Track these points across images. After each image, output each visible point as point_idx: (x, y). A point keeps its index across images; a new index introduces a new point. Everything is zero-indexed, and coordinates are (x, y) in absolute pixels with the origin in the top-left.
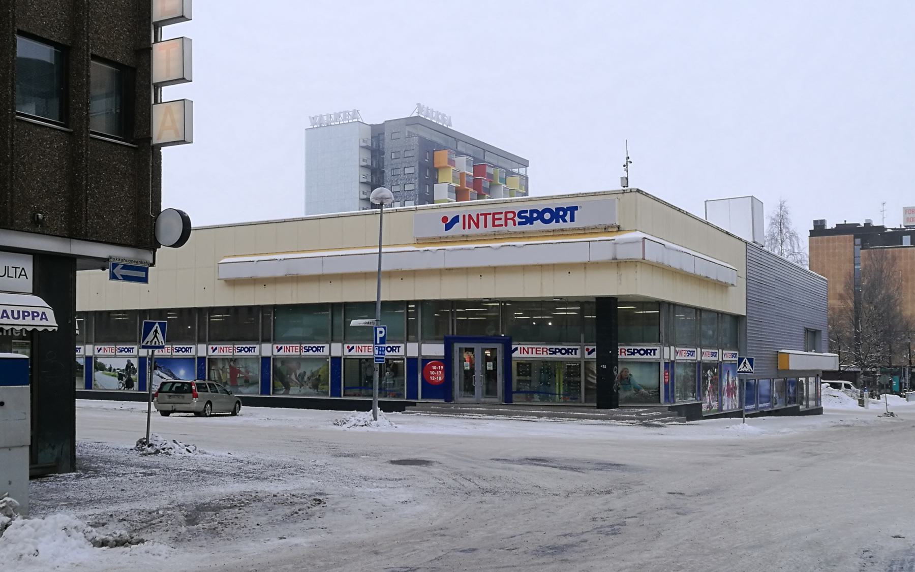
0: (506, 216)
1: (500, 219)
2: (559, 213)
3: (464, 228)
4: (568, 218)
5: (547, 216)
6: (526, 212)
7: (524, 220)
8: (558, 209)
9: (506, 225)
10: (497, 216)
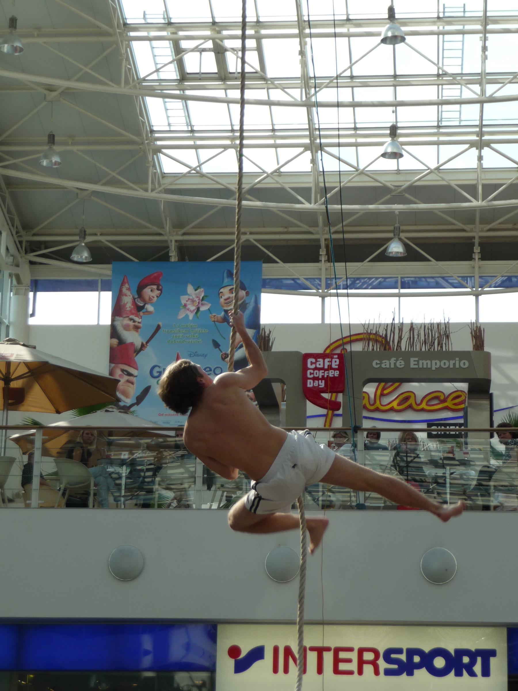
1: (349, 661)
2: (462, 660)
3: (275, 670)
4: (478, 668)
5: (439, 663)
6: (399, 651)
7: (395, 667)
8: (460, 653)
9: (360, 672)
10: (342, 655)
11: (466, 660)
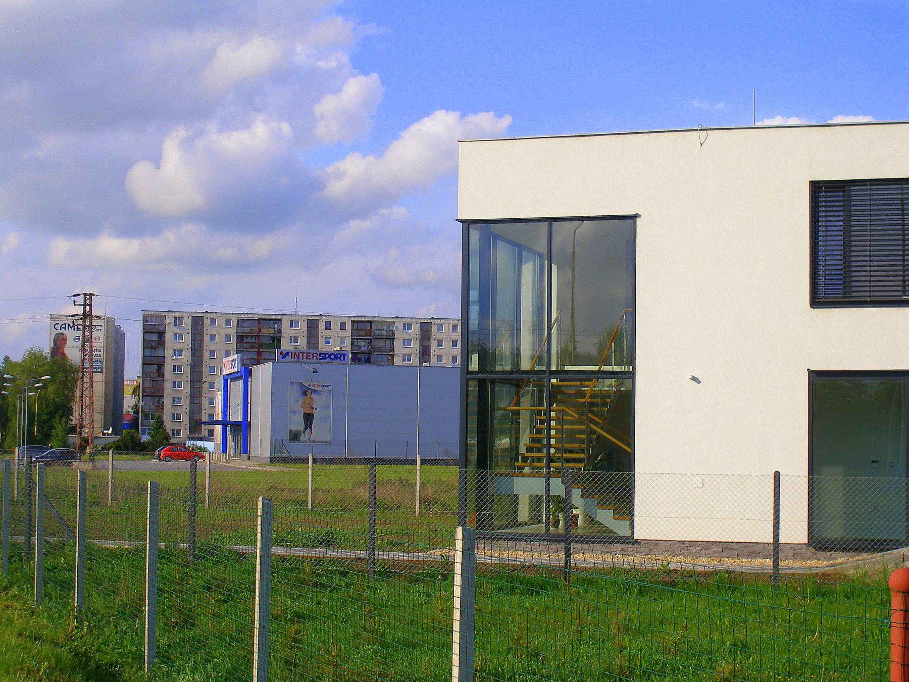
0: (313, 355)
3: (292, 358)
4: (342, 358)
5: (333, 357)
6: (323, 354)
8: (338, 354)
10: (308, 354)
11: (339, 356)
